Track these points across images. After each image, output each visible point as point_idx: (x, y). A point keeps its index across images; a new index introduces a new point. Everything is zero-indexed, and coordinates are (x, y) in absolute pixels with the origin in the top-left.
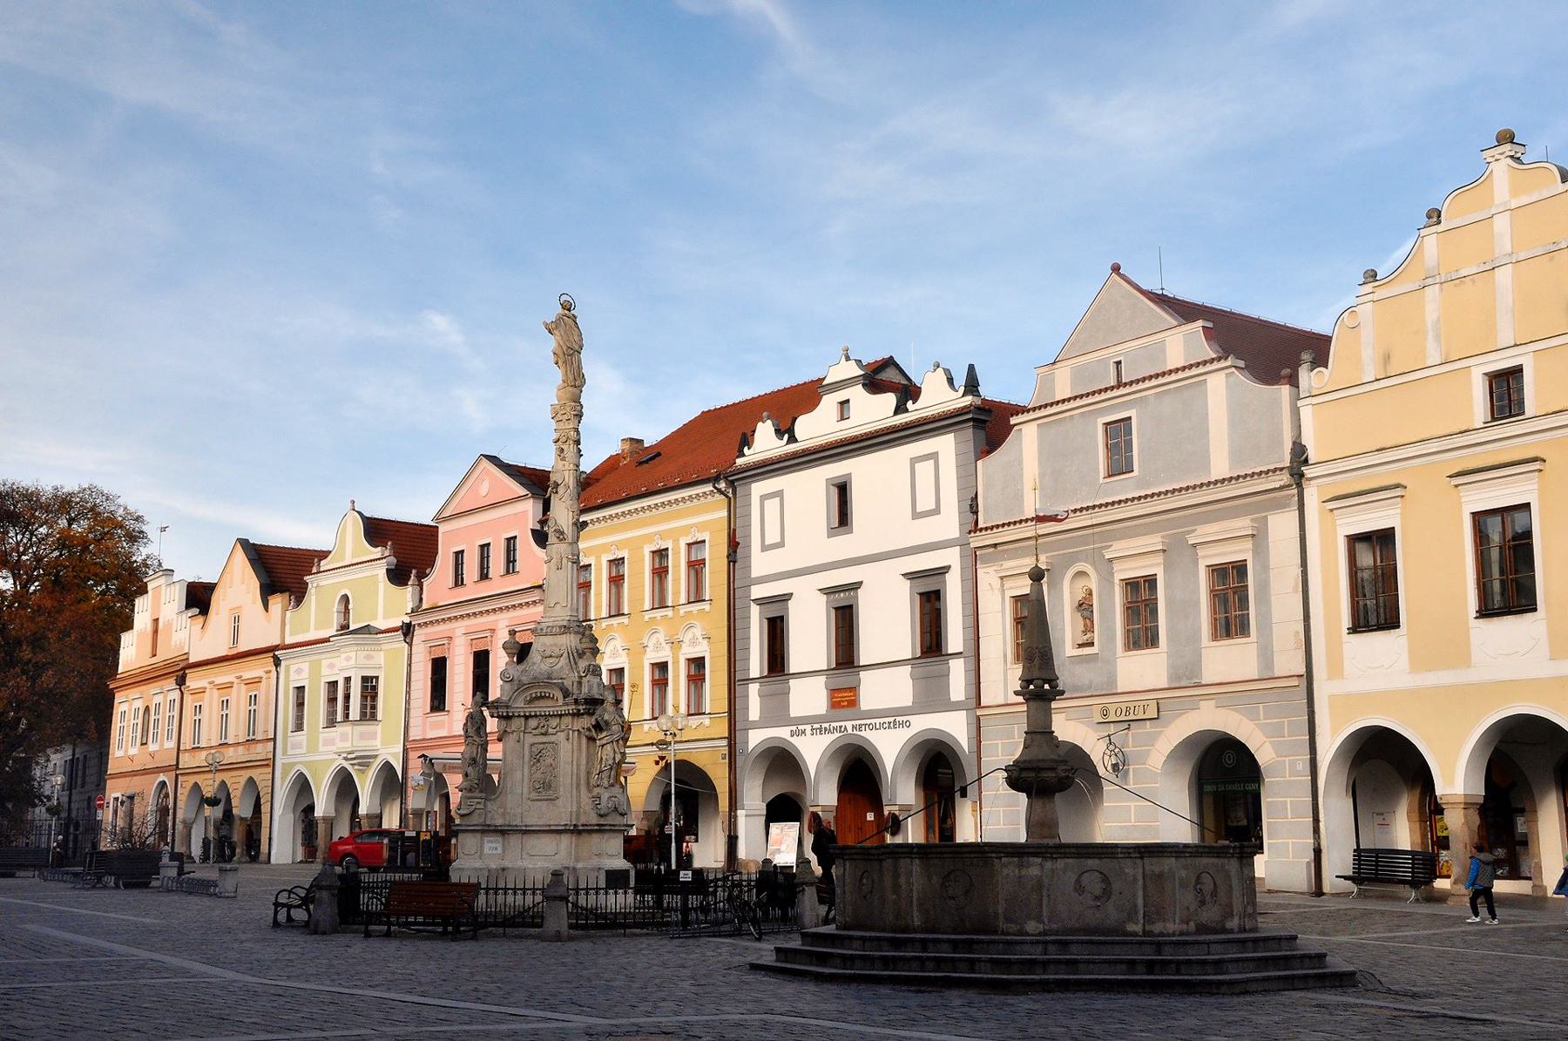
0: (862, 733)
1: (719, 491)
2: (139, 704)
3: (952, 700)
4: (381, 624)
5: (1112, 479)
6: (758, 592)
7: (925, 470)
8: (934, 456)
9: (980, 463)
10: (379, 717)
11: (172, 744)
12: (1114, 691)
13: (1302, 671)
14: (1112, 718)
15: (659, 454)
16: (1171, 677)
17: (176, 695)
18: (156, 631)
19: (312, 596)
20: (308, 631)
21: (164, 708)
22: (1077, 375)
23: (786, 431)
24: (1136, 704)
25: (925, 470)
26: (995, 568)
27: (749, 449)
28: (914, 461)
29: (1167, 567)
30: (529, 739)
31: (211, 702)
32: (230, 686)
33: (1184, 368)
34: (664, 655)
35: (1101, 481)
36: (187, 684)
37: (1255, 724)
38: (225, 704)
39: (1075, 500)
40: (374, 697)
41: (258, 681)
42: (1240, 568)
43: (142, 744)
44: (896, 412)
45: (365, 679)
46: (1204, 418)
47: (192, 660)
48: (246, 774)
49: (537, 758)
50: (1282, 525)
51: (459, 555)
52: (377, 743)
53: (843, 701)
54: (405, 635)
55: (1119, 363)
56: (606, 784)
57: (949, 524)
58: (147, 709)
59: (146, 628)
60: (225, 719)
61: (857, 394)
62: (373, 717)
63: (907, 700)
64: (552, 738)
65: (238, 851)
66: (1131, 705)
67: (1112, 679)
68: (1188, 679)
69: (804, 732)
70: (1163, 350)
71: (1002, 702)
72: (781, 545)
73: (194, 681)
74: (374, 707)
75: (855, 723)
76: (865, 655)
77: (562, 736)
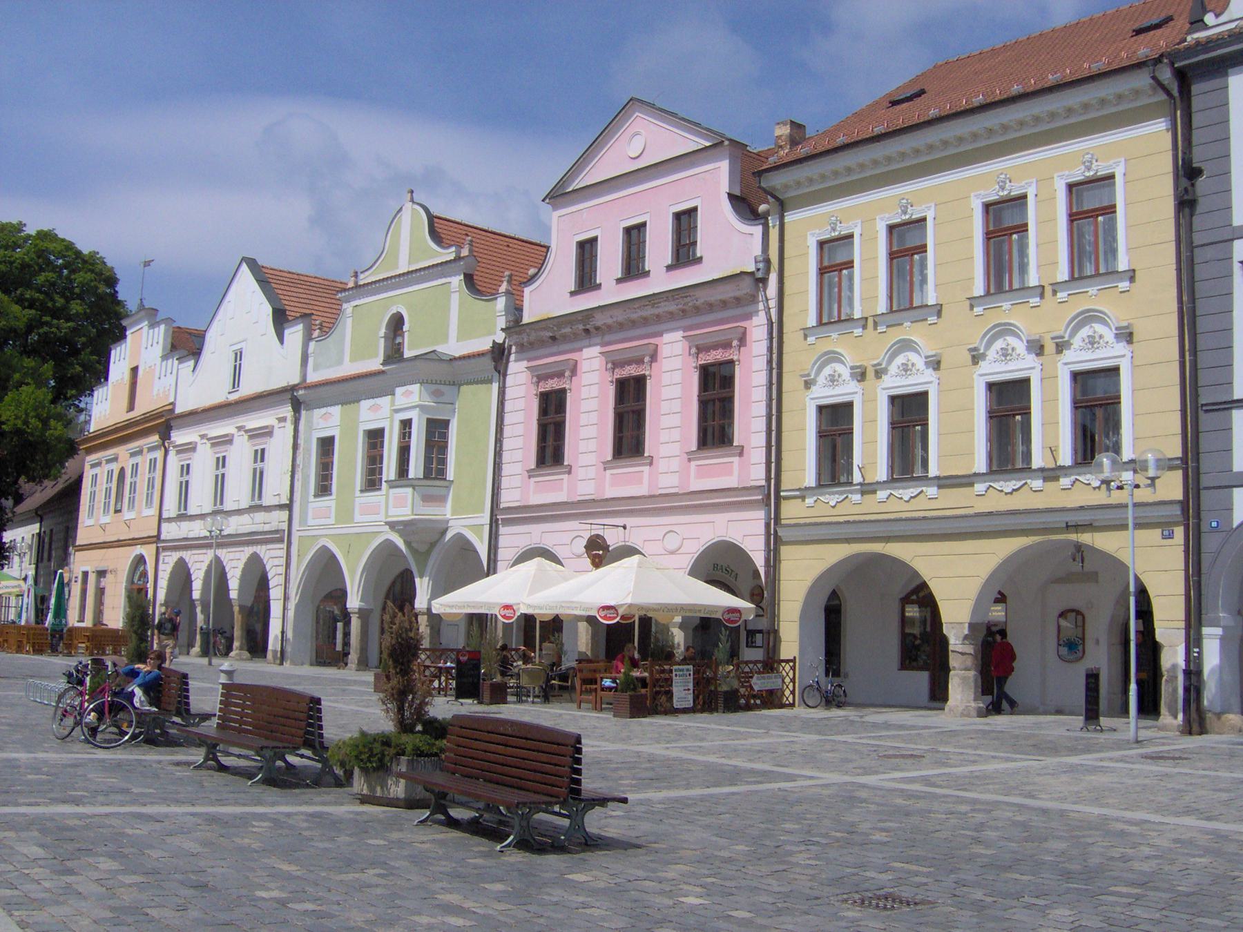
2: (115, 467)
4: (454, 347)
10: (451, 474)
11: (153, 511)
15: (921, 93)
17: (159, 454)
20: (340, 362)
31: (203, 461)
32: (227, 440)
36: (172, 439)
40: (443, 448)
41: (267, 432)
43: (117, 511)
45: (430, 422)
47: (178, 410)
48: (248, 551)
52: (446, 511)
54: (494, 360)
58: (122, 469)
59: (122, 379)
60: (220, 482)
62: (441, 473)
65: (236, 644)
73: (180, 437)
74: (443, 462)
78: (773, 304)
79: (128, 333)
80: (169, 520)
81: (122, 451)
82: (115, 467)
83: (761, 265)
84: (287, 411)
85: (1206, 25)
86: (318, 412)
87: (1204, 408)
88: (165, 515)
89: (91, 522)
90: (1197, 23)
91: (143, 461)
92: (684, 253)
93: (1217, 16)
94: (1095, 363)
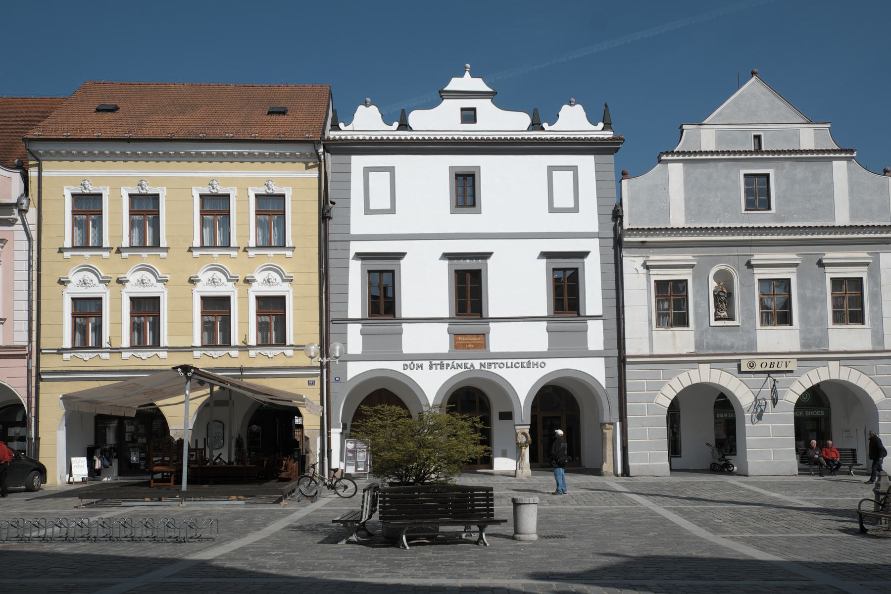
0: (492, 370)
3: (589, 349)
5: (749, 212)
8: (574, 169)
12: (754, 351)
14: (758, 368)
16: (803, 345)
24: (780, 361)
25: (563, 180)
28: (551, 169)
29: (799, 276)
33: (811, 151)
35: (743, 211)
39: (718, 221)
44: (528, 130)
53: (468, 344)
63: (544, 347)
66: (776, 361)
67: (753, 343)
68: (816, 347)
69: (421, 367)
71: (646, 352)
72: (392, 211)
75: (483, 361)
85: (341, 129)
87: (333, 322)
93: (345, 126)
94: (278, 293)
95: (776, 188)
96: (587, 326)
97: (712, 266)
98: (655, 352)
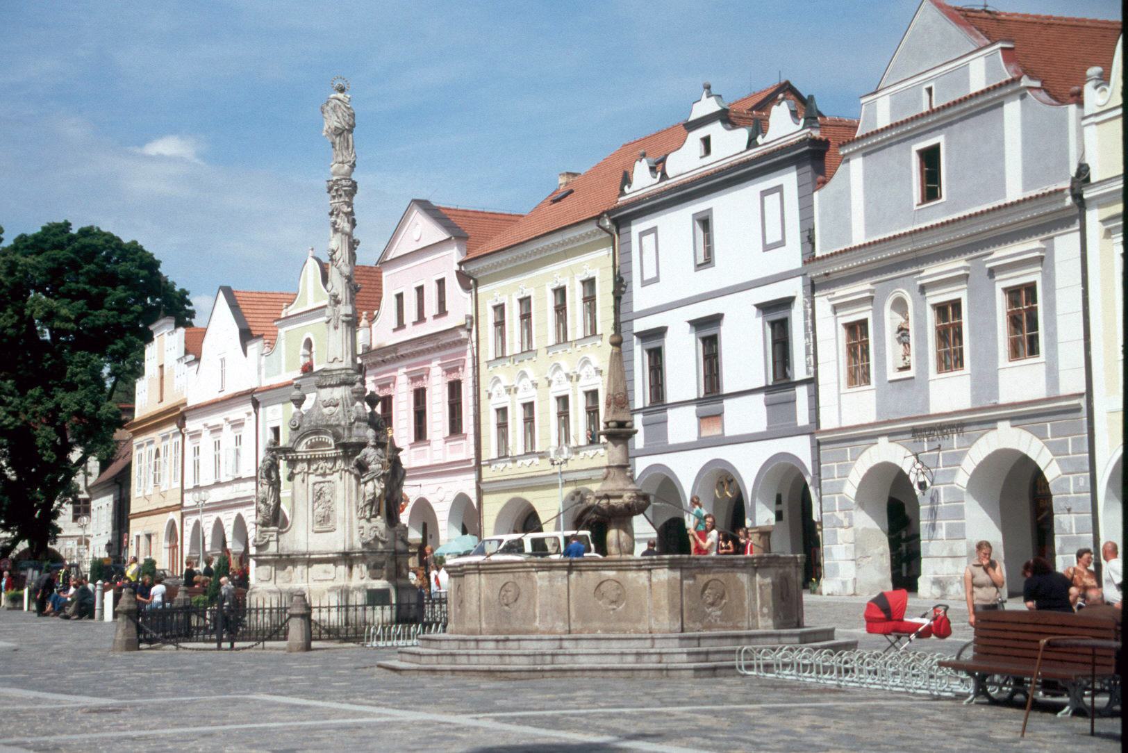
1: (604, 229)
2: (153, 448)
6: (640, 325)
7: (772, 200)
8: (779, 189)
9: (816, 194)
11: (179, 485)
12: (926, 413)
13: (1083, 389)
15: (571, 192)
18: (162, 378)
19: (282, 344)
20: (279, 373)
21: (171, 449)
22: (894, 107)
23: (658, 167)
26: (830, 297)
27: (629, 187)
28: (764, 193)
30: (312, 479)
32: (216, 429)
34: (564, 388)
37: (1044, 443)
38: (217, 445)
42: (1031, 289)
46: (1001, 143)
47: (189, 404)
48: (235, 512)
49: (319, 495)
50: (1065, 244)
51: (400, 297)
55: (930, 90)
56: (368, 516)
57: (791, 257)
58: (158, 450)
60: (217, 460)
61: (716, 130)
63: (761, 425)
64: (329, 478)
70: (967, 74)
71: (836, 425)
72: (656, 280)
73: (191, 425)
76: (727, 388)
77: (337, 475)
78: (474, 344)
79: (155, 337)
80: (189, 491)
81: (155, 435)
82: (153, 448)
83: (469, 321)
84: (250, 408)
86: (269, 409)
88: (186, 487)
89: (141, 494)
90: (622, 193)
91: (170, 443)
92: (442, 312)
95: (948, 163)
96: (795, 395)
97: (886, 295)
98: (844, 425)
